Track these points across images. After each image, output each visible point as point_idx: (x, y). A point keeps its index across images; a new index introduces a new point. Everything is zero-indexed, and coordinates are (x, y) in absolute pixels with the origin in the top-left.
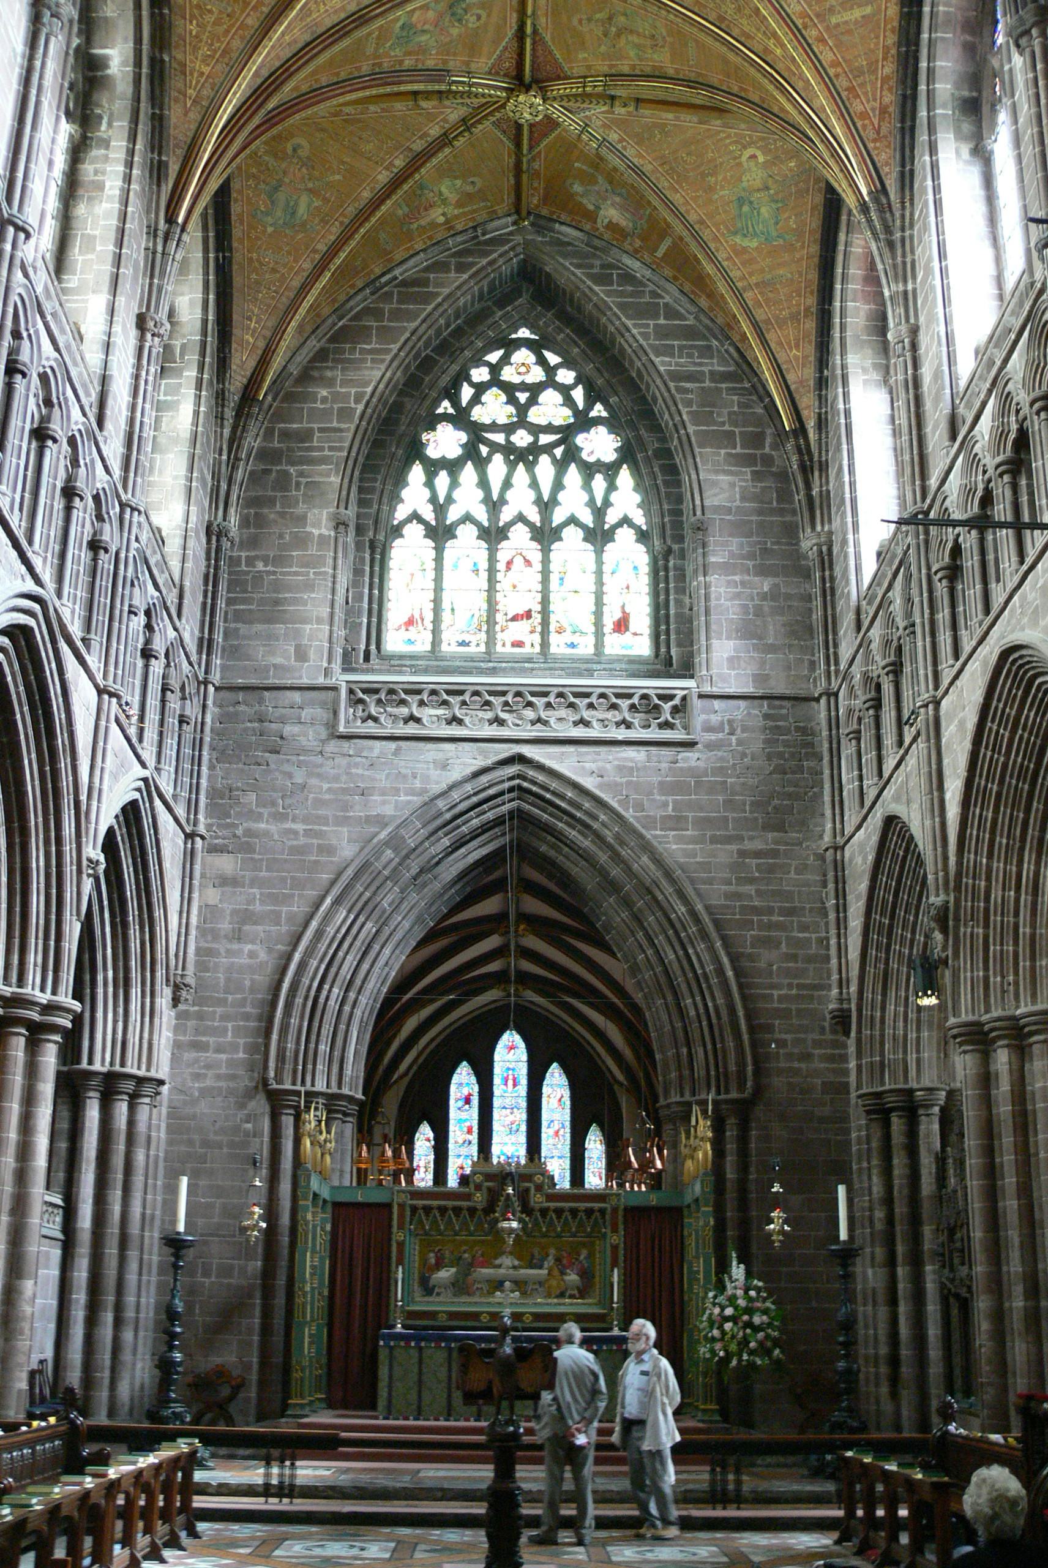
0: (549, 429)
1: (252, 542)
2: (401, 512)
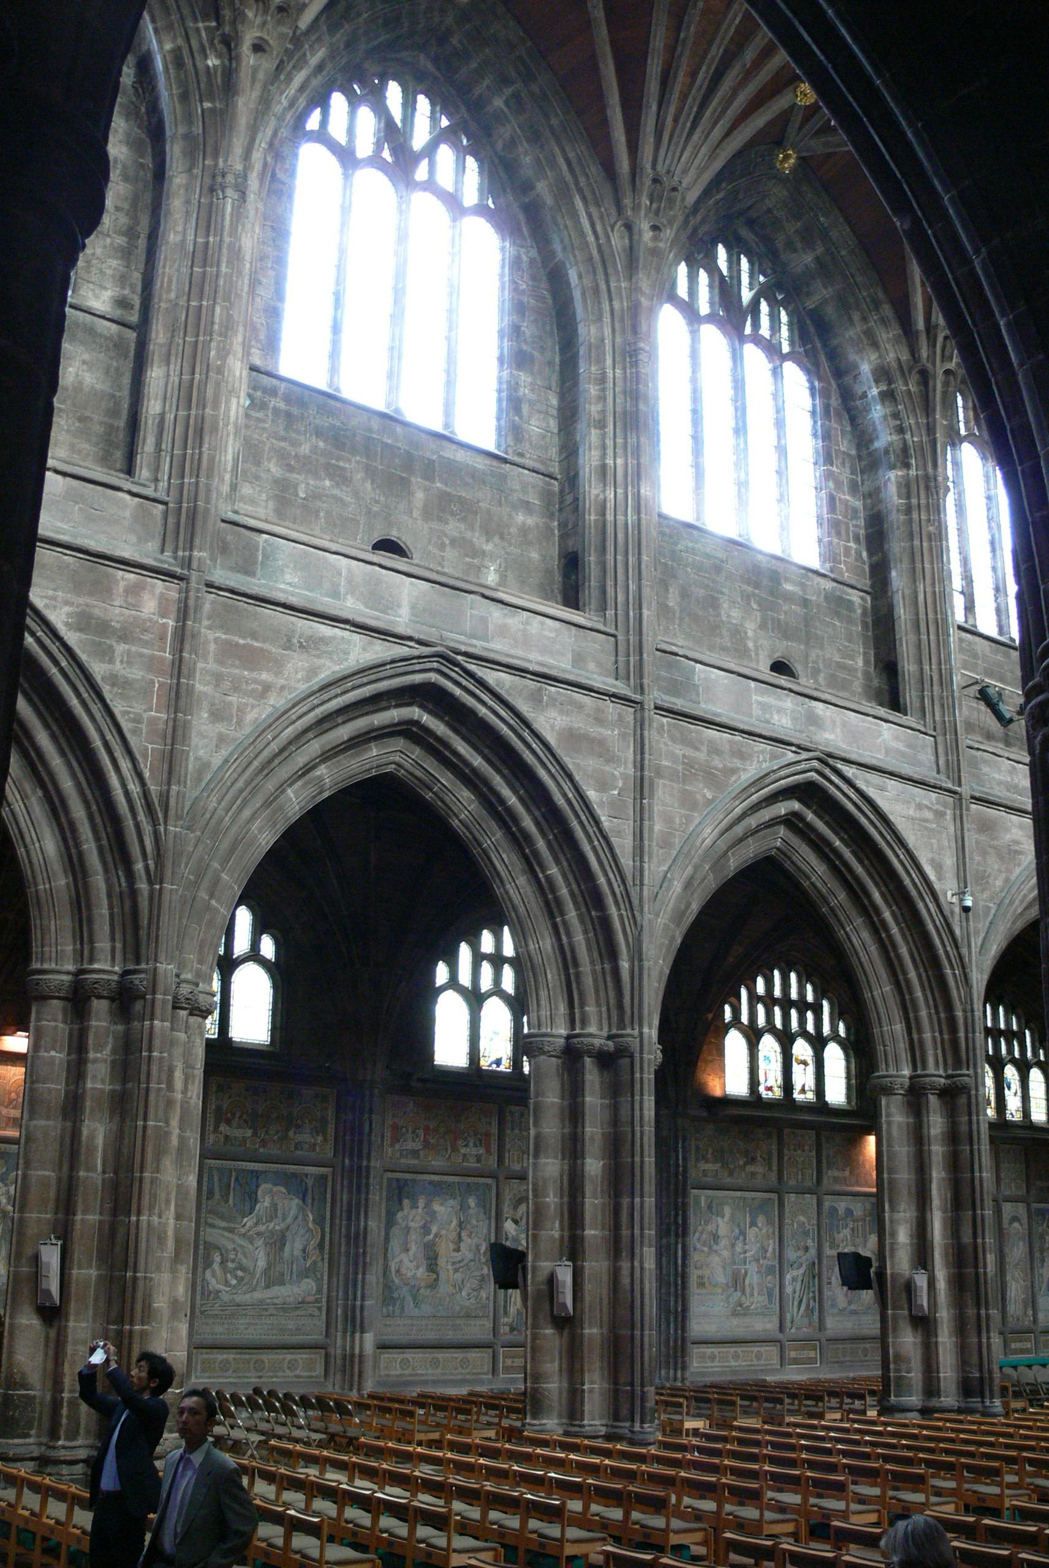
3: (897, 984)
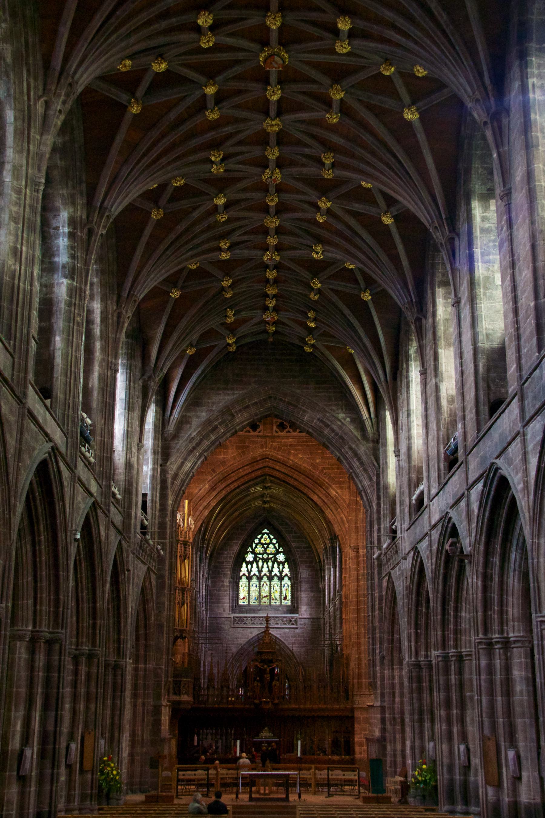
0: (271, 554)
1: (214, 586)
2: (241, 574)
3: (35, 576)
